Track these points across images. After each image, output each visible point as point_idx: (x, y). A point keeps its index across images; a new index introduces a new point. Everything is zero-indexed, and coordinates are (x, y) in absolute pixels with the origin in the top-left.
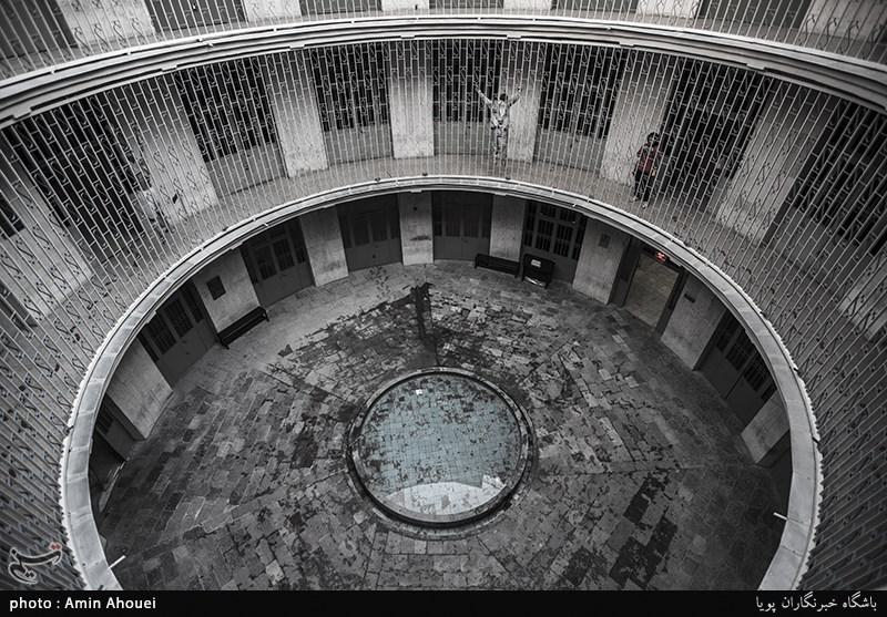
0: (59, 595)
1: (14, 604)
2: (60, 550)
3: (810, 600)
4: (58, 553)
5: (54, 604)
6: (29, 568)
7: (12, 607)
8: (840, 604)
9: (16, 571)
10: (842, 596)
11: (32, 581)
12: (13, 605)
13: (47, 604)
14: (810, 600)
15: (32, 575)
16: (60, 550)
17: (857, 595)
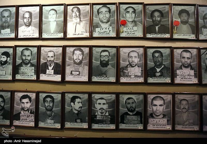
4: (13, 129)
5: (13, 141)
7: (4, 142)
11: (8, 136)
12: (5, 141)
13: (11, 141)
15: (7, 134)
16: (14, 128)
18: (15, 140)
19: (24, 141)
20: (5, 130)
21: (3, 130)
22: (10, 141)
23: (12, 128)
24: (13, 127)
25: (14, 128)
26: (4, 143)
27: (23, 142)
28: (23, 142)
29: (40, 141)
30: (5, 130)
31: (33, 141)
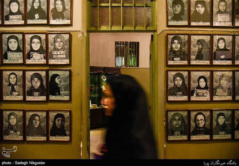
0: (13, 161)
1: (3, 163)
2: (16, 148)
3: (218, 162)
4: (16, 149)
5: (12, 163)
6: (8, 153)
7: (2, 164)
8: (226, 163)
9: (4, 154)
10: (227, 161)
11: (9, 156)
12: (3, 163)
13: (10, 163)
14: (218, 162)
15: (9, 155)
16: (16, 148)
17: (231, 161)
20: (6, 150)
21: (4, 150)
22: (9, 163)
24: (15, 146)
25: (16, 147)
26: (2, 165)
30: (6, 150)
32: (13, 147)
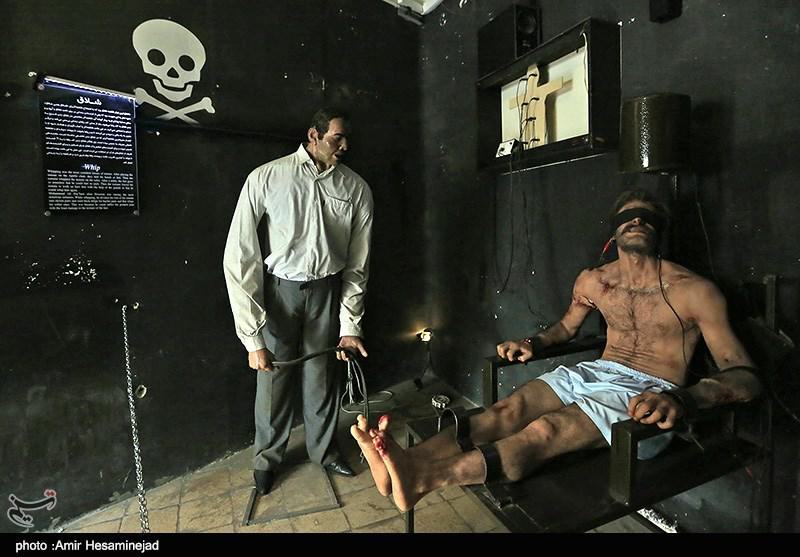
2: (55, 497)
4: (52, 500)
5: (50, 547)
7: (17, 549)
9: (14, 516)
11: (27, 525)
12: (20, 546)
13: (44, 546)
15: (29, 519)
16: (55, 497)
18: (59, 542)
19: (92, 545)
20: (19, 505)
21: (13, 502)
23: (48, 494)
27: (90, 547)
28: (90, 547)
29: (155, 546)
30: (19, 505)
31: (127, 546)
32: (45, 494)
